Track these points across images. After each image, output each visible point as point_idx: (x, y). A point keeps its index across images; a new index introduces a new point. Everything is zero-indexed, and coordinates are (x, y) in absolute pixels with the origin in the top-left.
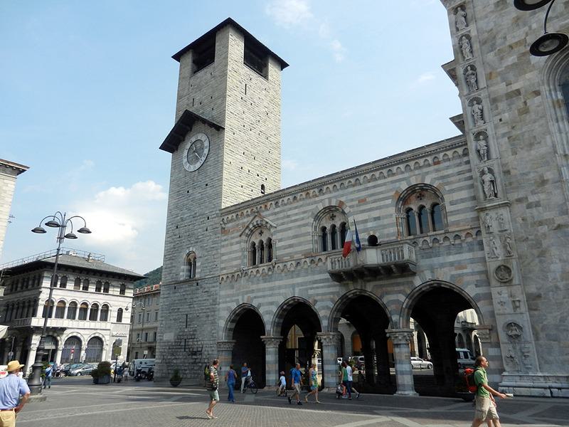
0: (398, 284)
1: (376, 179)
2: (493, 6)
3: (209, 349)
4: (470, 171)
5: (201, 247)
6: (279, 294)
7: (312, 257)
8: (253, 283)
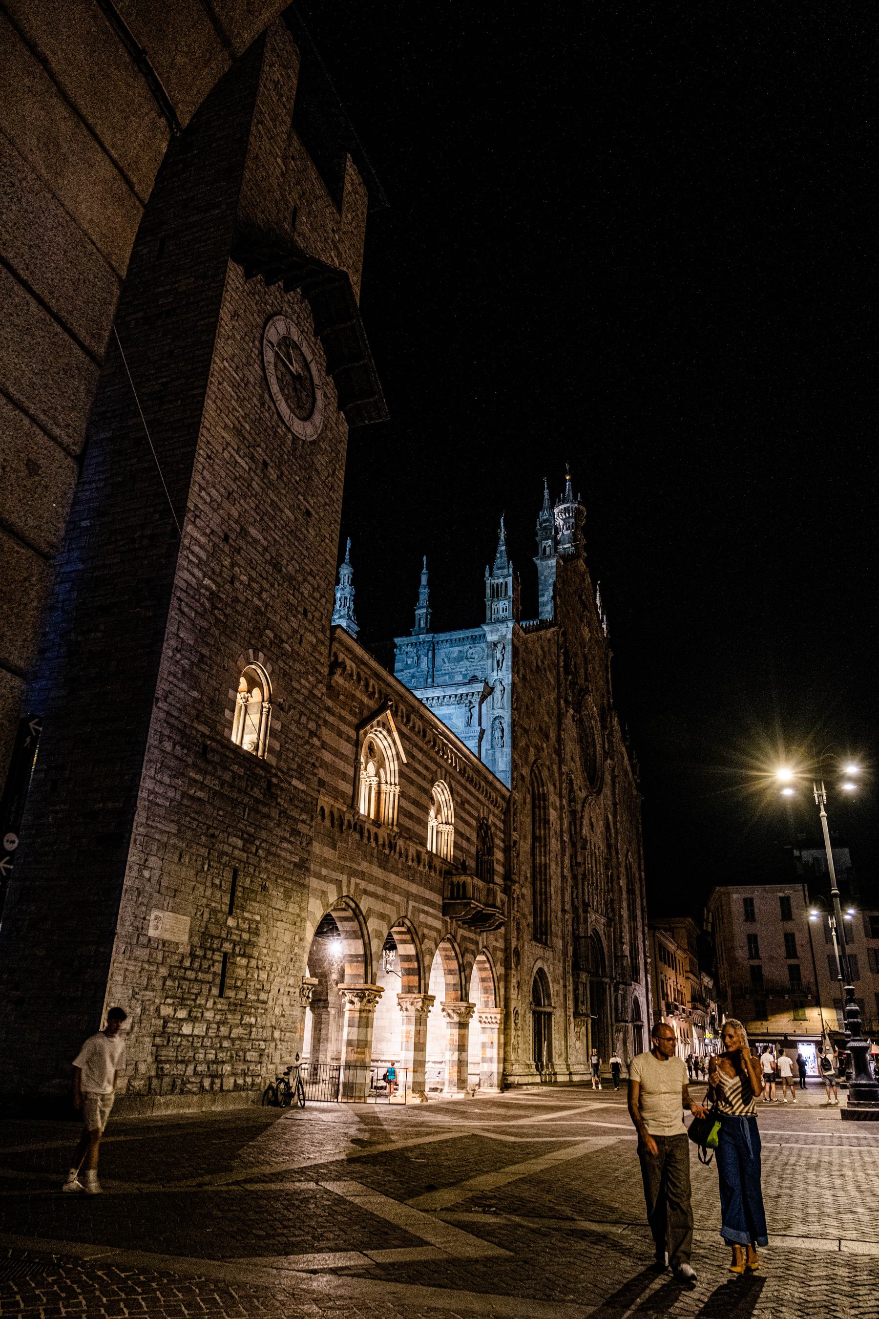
6: (393, 903)
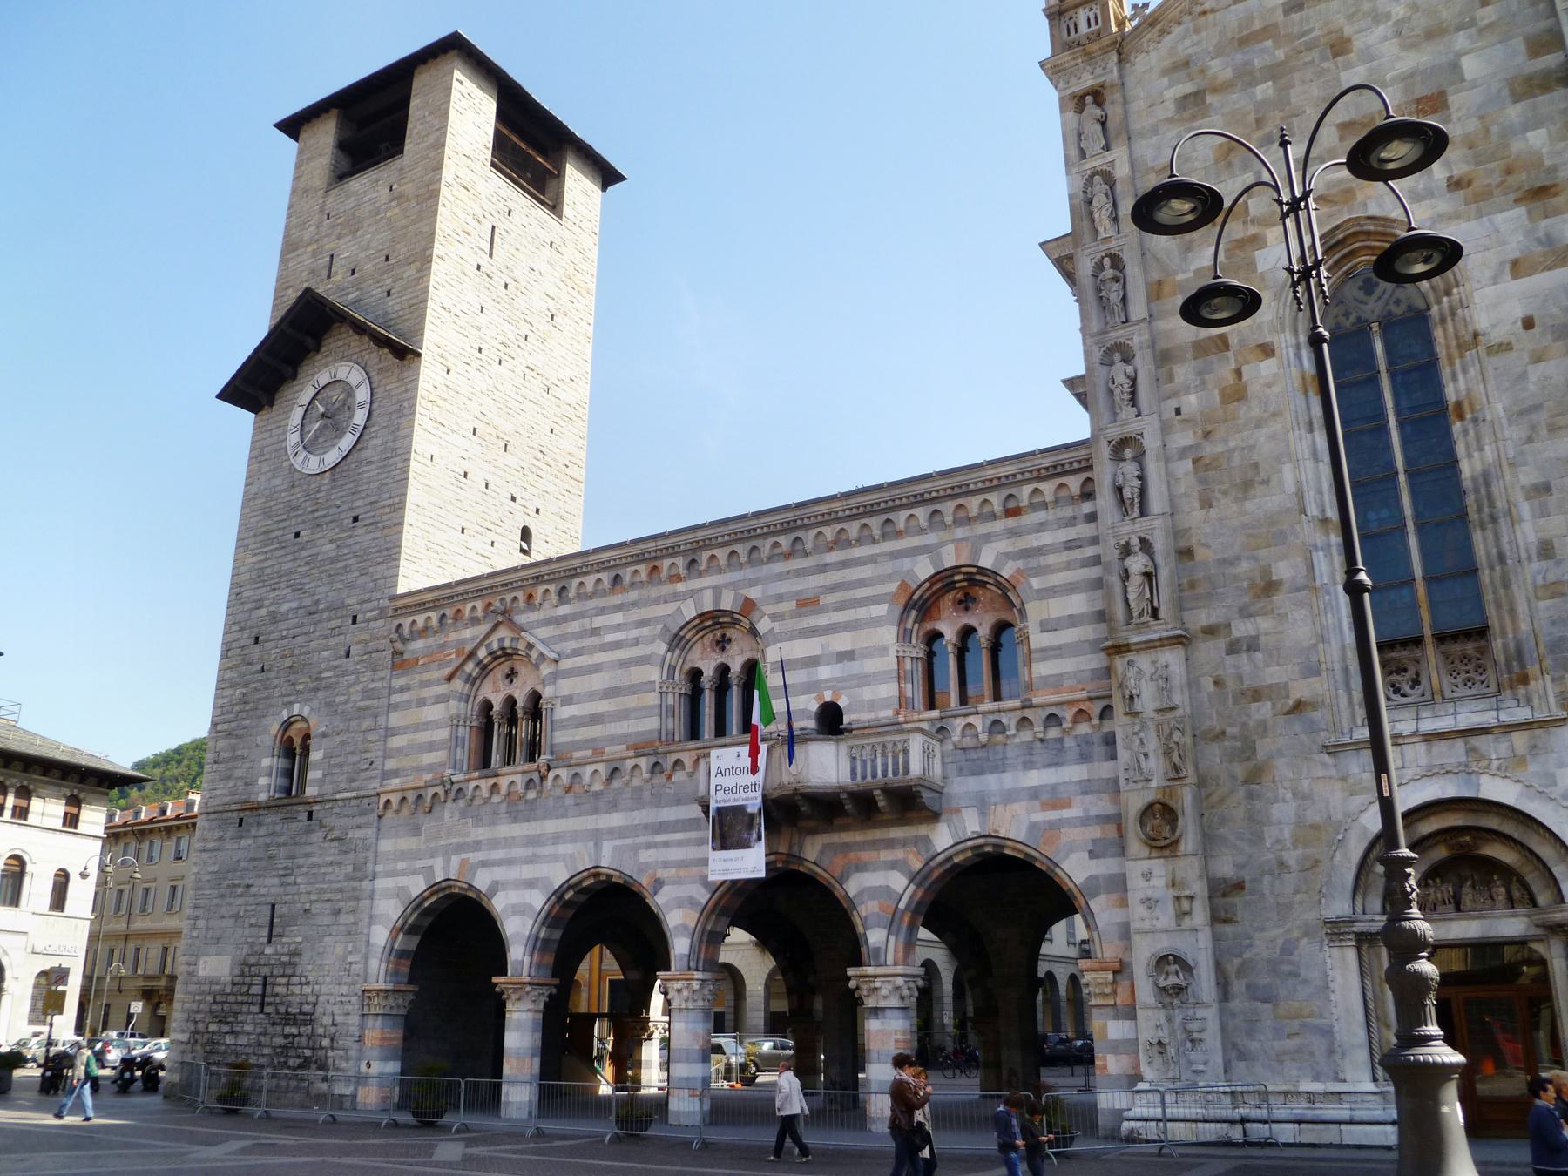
0: (890, 844)
1: (848, 544)
2: (1172, 106)
3: (336, 1009)
4: (1095, 541)
5: (328, 705)
6: (555, 858)
7: (657, 754)
8: (478, 821)
